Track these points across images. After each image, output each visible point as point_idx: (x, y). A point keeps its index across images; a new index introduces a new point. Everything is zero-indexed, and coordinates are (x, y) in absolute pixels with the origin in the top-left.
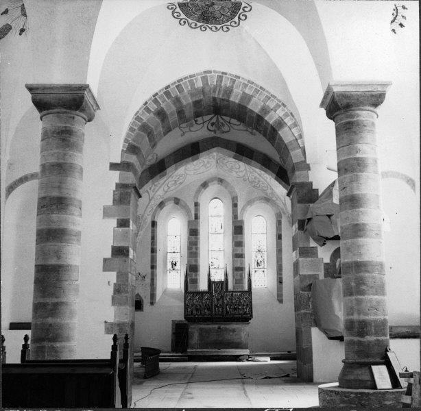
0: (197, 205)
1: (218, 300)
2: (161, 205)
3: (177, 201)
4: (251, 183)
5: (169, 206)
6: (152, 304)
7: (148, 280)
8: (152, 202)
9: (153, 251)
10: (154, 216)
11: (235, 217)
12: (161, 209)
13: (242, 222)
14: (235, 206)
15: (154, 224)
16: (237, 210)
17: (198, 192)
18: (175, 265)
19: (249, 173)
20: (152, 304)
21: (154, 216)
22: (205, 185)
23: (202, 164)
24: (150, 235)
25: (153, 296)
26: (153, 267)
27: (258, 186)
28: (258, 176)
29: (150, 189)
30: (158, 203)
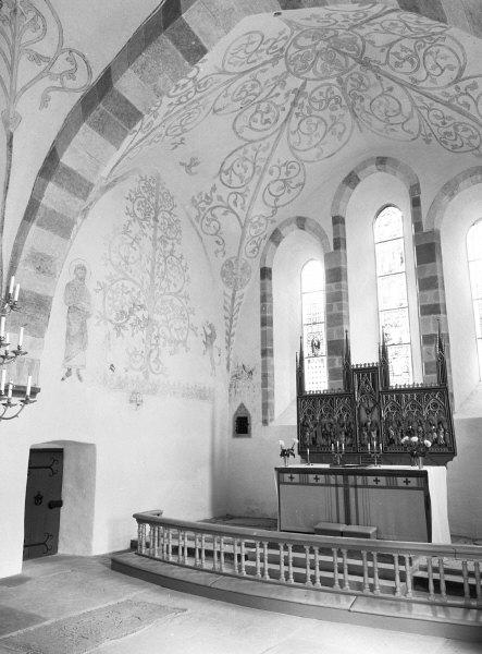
0: (338, 221)
1: (369, 411)
2: (276, 237)
3: (301, 222)
4: (443, 142)
5: (292, 236)
6: (265, 422)
7: (257, 378)
8: (251, 231)
9: (266, 322)
10: (263, 259)
11: (418, 226)
12: (277, 244)
13: (435, 234)
14: (416, 203)
15: (265, 273)
16: (420, 213)
17: (339, 196)
18: (318, 347)
19: (424, 112)
20: (265, 422)
21: (263, 259)
22: (352, 180)
23: (321, 129)
24: (258, 293)
25: (266, 407)
26: (266, 352)
27: (459, 143)
28: (448, 112)
29: (235, 203)
30: (269, 232)
